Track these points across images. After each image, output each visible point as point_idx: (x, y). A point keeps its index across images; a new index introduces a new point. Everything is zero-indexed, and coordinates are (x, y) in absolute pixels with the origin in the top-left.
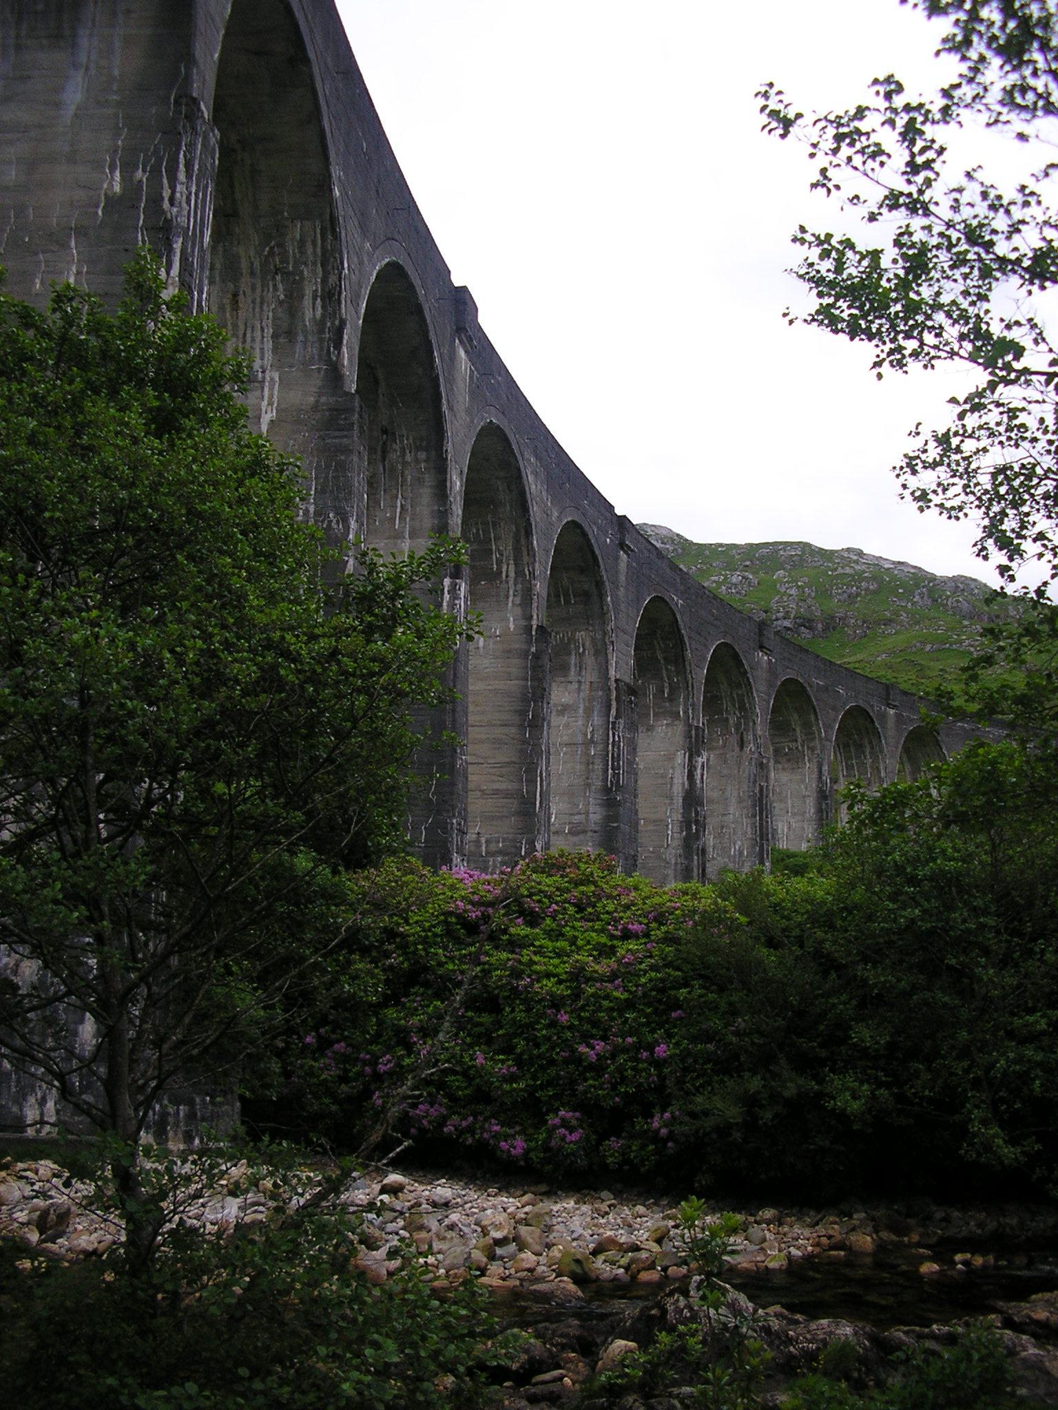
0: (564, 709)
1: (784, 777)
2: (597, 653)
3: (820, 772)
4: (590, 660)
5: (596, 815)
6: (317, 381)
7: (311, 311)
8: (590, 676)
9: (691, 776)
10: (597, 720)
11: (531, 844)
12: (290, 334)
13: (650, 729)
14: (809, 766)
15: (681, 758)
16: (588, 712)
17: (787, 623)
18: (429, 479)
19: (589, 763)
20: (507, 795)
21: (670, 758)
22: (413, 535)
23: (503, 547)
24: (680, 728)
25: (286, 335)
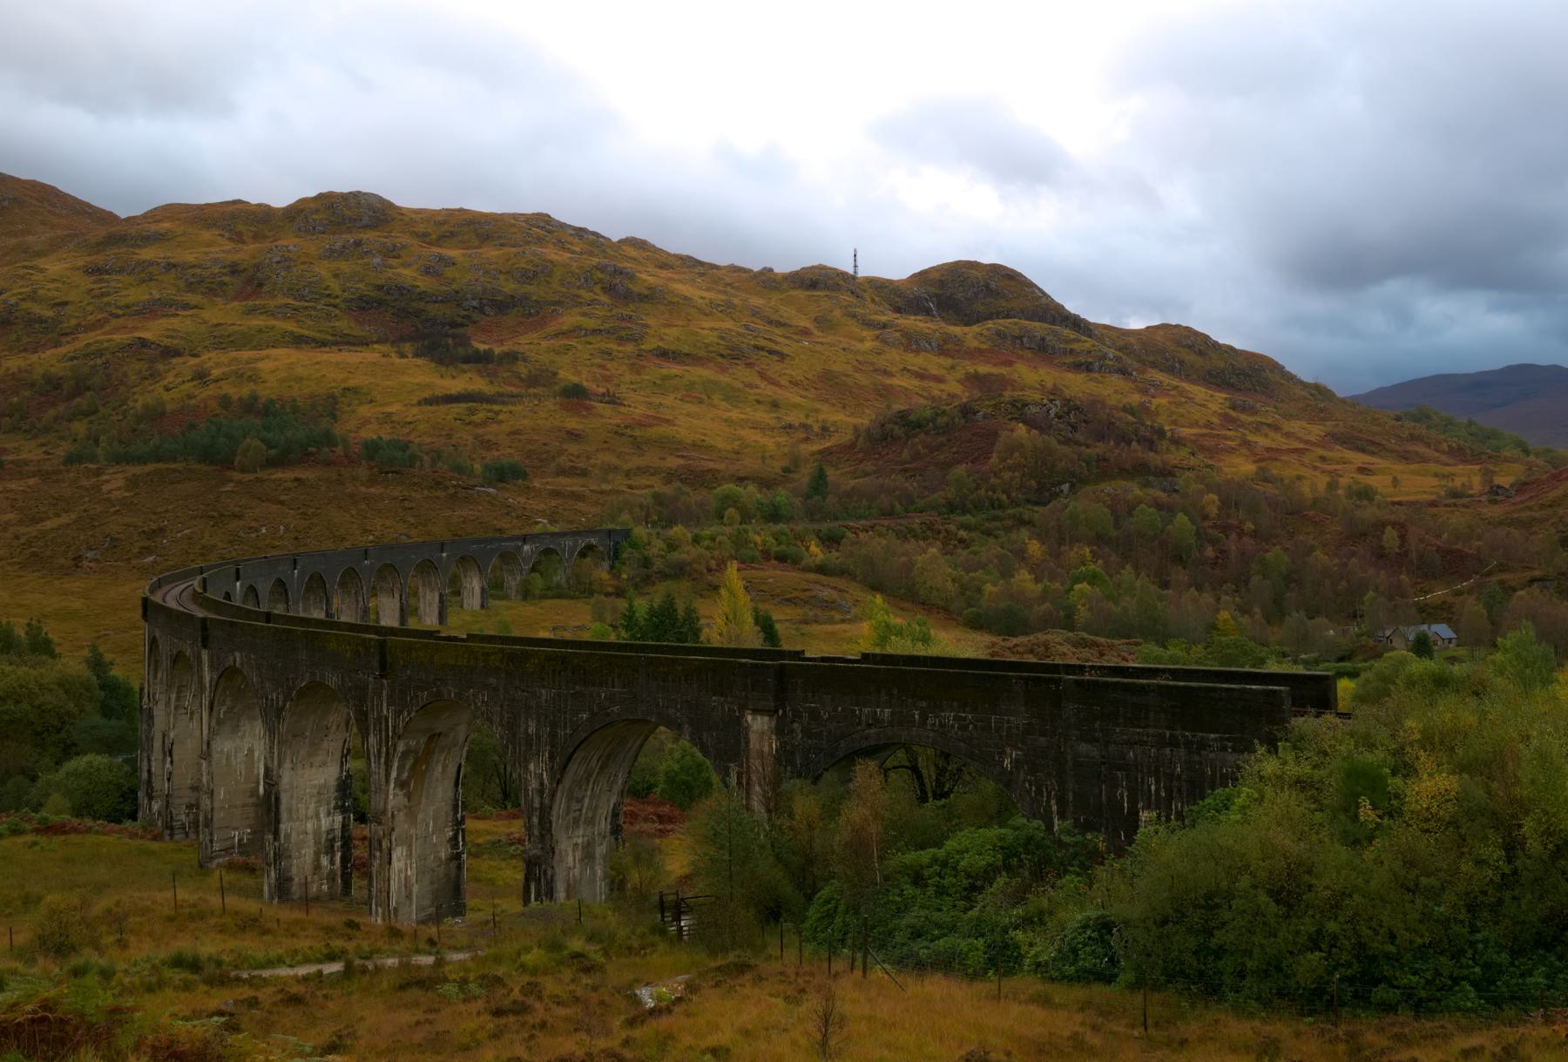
17: (475, 303)
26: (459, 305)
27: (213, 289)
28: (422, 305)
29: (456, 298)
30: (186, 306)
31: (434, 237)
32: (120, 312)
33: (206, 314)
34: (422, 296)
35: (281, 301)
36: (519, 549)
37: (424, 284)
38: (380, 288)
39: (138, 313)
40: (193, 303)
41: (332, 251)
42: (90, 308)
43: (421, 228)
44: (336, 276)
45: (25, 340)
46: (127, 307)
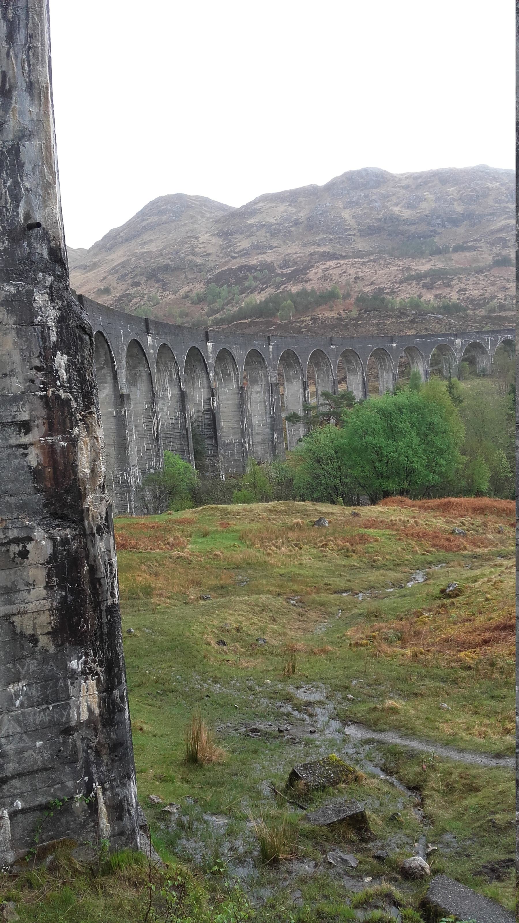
0: (258, 392)
1: (351, 378)
2: (265, 377)
3: (363, 376)
4: (263, 379)
5: (269, 420)
6: (177, 389)
7: (175, 377)
8: (264, 383)
9: (305, 396)
10: (267, 395)
11: (244, 440)
12: (171, 381)
13: (292, 383)
14: (359, 374)
15: (301, 391)
16: (264, 393)
17: (439, 221)
18: (205, 376)
19: (266, 406)
20: (237, 428)
21: (298, 391)
22: (203, 388)
23: (230, 368)
24: (301, 382)
25: (171, 380)
26: (429, 224)
27: (288, 236)
28: (406, 227)
29: (426, 220)
30: (271, 248)
31: (414, 187)
32: (236, 255)
33: (280, 250)
34: (406, 222)
35: (322, 236)
36: (452, 342)
37: (407, 214)
38: (379, 220)
39: (246, 254)
40: (275, 245)
41: (351, 202)
42: (221, 255)
43: (404, 183)
44: (354, 217)
45: (190, 276)
46: (240, 251)
